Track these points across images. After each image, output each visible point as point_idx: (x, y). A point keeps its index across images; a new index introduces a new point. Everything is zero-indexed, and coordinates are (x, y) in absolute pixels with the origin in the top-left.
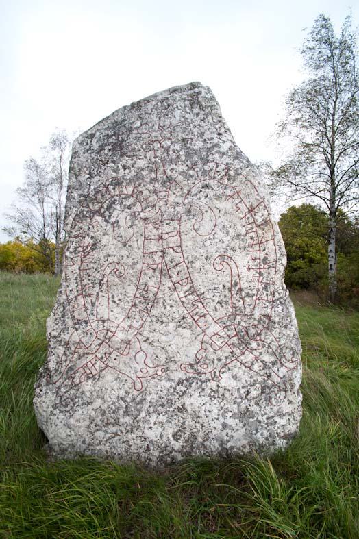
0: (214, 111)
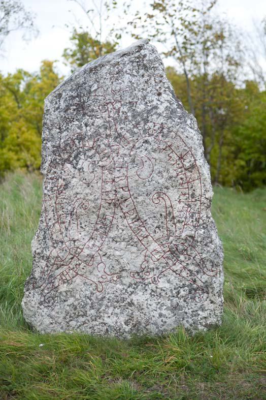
0: (157, 72)
